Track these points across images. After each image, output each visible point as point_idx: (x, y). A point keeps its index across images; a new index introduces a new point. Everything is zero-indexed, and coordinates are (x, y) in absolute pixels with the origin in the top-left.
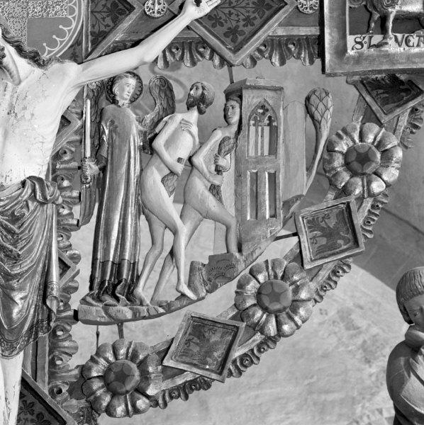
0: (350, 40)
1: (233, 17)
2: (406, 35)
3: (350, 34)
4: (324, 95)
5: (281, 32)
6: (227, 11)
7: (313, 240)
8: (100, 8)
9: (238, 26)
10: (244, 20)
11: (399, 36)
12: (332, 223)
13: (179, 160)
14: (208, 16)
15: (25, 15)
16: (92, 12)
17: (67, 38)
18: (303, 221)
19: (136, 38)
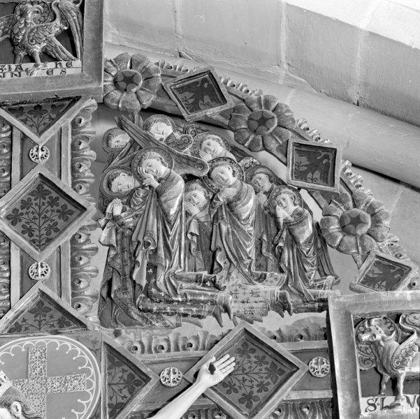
0: (363, 402)
1: (247, 383)
3: (363, 396)
5: (295, 396)
6: (240, 378)
8: (117, 380)
9: (252, 392)
10: (257, 386)
11: (411, 397)
14: (223, 383)
15: (44, 391)
16: (109, 384)
19: (153, 408)
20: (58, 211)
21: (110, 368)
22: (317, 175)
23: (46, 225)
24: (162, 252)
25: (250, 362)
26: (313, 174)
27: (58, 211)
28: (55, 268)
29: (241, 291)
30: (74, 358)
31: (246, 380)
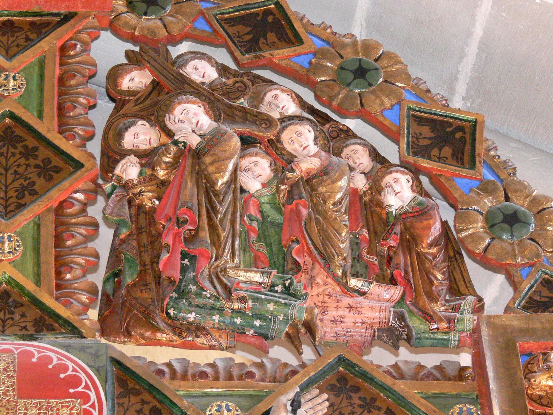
20: (37, 166)
21: (120, 396)
22: (447, 151)
23: (17, 184)
24: (205, 234)
25: (352, 405)
26: (440, 150)
27: (37, 166)
28: (30, 242)
29: (331, 303)
30: (62, 376)
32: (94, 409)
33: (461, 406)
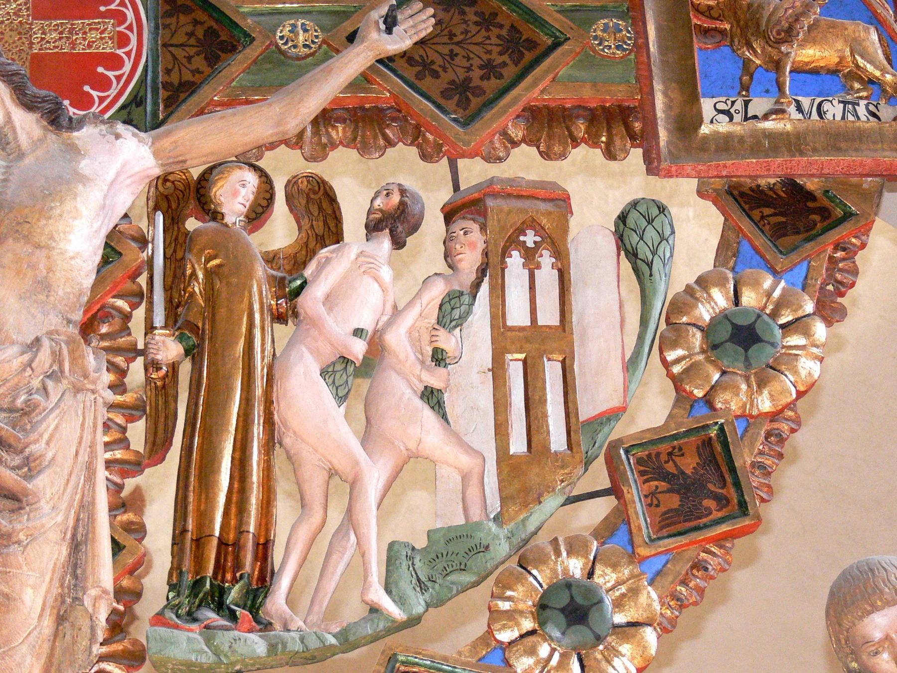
0: (707, 106)
1: (458, 60)
2: (818, 100)
4: (654, 211)
6: (445, 50)
7: (652, 500)
8: (180, 38)
9: (468, 80)
10: (481, 67)
12: (689, 463)
13: (358, 332)
15: (25, 47)
16: (165, 45)
17: (113, 92)
18: (628, 459)
21: (167, 14)
25: (465, 22)
31: (457, 55)
32: (132, 32)
33: (606, 21)
